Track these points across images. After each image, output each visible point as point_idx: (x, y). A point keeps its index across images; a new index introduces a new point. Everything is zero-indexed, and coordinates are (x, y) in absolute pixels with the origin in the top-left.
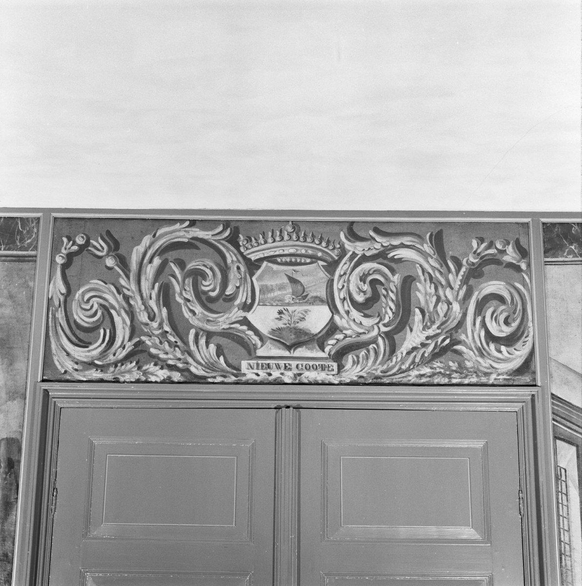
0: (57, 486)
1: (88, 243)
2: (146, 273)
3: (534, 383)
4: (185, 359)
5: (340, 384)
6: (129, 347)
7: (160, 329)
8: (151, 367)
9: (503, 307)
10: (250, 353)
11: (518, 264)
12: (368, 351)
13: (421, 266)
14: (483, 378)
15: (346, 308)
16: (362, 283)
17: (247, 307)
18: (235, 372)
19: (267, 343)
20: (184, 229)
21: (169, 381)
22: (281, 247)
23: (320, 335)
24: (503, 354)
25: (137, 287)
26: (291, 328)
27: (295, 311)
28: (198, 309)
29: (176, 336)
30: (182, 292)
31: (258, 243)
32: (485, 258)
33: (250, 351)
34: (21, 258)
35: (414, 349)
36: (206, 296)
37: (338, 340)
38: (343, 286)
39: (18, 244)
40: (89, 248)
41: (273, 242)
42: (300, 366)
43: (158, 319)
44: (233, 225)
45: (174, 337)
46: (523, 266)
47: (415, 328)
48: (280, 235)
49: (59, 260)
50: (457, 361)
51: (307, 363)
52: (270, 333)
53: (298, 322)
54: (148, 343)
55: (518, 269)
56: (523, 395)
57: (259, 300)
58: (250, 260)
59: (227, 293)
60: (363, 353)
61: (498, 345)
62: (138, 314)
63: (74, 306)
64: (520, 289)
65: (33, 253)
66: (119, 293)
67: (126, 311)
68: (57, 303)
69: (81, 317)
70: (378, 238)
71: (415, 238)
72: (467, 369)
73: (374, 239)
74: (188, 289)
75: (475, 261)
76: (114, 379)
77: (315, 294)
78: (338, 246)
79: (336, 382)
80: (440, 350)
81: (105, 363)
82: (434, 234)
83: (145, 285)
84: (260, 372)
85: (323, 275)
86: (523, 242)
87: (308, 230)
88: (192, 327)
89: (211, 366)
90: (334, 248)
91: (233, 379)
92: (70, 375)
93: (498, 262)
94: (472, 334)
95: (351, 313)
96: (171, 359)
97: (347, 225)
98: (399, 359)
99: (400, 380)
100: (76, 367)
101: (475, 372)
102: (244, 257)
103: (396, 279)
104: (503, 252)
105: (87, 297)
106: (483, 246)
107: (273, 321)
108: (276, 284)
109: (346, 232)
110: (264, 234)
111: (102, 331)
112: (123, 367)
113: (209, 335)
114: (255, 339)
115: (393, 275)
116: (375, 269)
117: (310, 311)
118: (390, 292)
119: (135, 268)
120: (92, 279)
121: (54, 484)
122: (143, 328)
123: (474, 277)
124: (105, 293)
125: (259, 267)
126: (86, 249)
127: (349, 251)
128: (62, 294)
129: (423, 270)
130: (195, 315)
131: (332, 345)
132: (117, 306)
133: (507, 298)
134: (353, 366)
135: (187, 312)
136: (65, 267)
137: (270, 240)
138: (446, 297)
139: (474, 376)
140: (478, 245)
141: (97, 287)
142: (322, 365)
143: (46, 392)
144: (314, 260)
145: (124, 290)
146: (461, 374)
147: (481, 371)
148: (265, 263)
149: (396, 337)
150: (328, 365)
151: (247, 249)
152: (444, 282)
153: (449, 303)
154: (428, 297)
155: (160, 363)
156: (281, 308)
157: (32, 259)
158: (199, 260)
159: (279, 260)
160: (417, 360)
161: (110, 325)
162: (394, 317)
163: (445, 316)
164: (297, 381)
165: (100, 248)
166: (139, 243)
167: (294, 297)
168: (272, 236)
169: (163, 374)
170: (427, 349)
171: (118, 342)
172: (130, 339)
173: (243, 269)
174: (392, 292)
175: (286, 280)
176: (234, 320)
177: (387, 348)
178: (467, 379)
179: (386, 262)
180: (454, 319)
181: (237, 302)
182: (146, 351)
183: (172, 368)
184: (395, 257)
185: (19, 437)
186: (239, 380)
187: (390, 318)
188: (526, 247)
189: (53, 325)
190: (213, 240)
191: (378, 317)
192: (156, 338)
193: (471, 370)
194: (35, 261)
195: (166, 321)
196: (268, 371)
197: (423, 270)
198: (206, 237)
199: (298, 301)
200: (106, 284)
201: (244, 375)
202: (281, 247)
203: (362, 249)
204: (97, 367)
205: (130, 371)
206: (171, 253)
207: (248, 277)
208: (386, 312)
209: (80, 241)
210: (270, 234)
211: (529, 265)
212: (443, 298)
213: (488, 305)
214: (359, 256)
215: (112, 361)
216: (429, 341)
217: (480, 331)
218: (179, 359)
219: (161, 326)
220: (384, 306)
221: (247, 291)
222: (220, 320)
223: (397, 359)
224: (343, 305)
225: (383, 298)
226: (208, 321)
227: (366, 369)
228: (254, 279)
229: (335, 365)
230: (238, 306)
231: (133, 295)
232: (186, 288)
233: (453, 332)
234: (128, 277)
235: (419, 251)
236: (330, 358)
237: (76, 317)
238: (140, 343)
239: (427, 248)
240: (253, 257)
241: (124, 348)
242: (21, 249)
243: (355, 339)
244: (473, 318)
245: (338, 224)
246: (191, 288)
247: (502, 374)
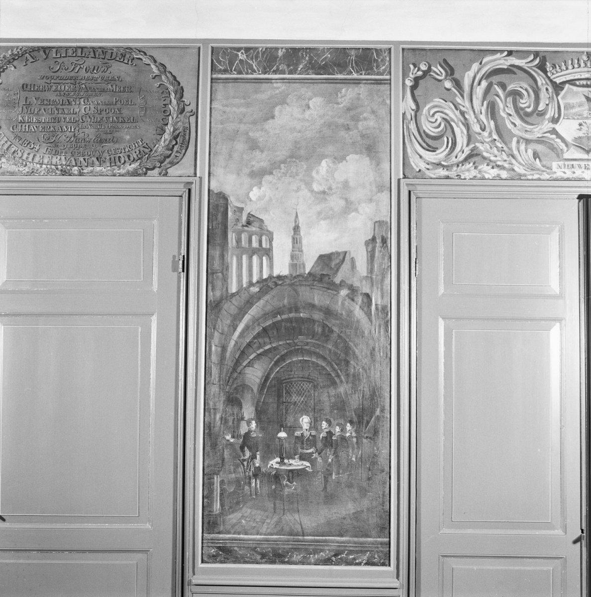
1: (429, 69)
2: (476, 94)
6: (467, 151)
8: (484, 167)
10: (558, 156)
17: (555, 120)
22: (579, 72)
25: (470, 103)
28: (518, 121)
29: (502, 143)
30: (505, 108)
33: (558, 154)
39: (375, 70)
43: (488, 129)
44: (541, 54)
48: (578, 63)
49: (409, 83)
52: (573, 140)
58: (555, 83)
59: (540, 109)
62: (472, 126)
65: (388, 77)
66: (457, 109)
67: (463, 124)
68: (409, 117)
69: (428, 128)
83: (477, 102)
84: (566, 171)
91: (548, 177)
96: (499, 161)
100: (428, 167)
102: (551, 81)
105: (432, 112)
108: (577, 103)
111: (445, 139)
112: (463, 167)
113: (528, 141)
114: (562, 146)
120: (435, 97)
122: (477, 137)
125: (562, 89)
128: (413, 110)
136: (414, 88)
137: (570, 67)
141: (439, 104)
145: (460, 106)
148: (567, 86)
151: (553, 74)
156: (581, 121)
158: (517, 83)
159: (578, 83)
166: (469, 69)
168: (572, 64)
172: (468, 145)
175: (584, 99)
176: (545, 131)
181: (547, 116)
189: (408, 134)
190: (527, 67)
195: (494, 132)
200: (446, 102)
202: (579, 72)
205: (468, 170)
206: (494, 77)
207: (555, 96)
209: (424, 67)
210: (570, 62)
219: (490, 134)
221: (555, 108)
222: (535, 130)
226: (526, 131)
228: (559, 97)
230: (549, 119)
232: (508, 105)
234: (462, 96)
237: (425, 128)
238: (475, 148)
240: (558, 81)
241: (463, 152)
242: (378, 74)
246: (512, 105)
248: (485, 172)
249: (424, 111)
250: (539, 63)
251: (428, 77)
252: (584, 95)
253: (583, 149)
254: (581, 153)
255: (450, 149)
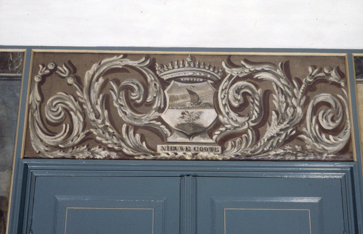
0: (33, 228)
1: (56, 69)
2: (94, 88)
3: (352, 160)
4: (120, 144)
5: (224, 160)
6: (82, 135)
7: (103, 124)
8: (97, 149)
9: (329, 110)
10: (163, 140)
11: (339, 82)
12: (242, 139)
13: (275, 84)
14: (318, 156)
15: (227, 110)
16: (237, 95)
17: (161, 110)
18: (153, 152)
19: (174, 133)
20: (120, 60)
21: (109, 158)
23: (210, 128)
24: (331, 141)
26: (190, 124)
27: (193, 112)
28: (128, 111)
30: (118, 101)
31: (168, 69)
32: (317, 79)
33: (163, 139)
34: (11, 78)
35: (272, 137)
36: (133, 103)
37: (222, 132)
38: (225, 96)
39: (10, 69)
40: (57, 72)
41: (177, 68)
42: (197, 148)
43: (102, 118)
45: (112, 129)
46: (342, 84)
47: (272, 124)
48: (183, 64)
49: (37, 79)
50: (301, 145)
51: (201, 146)
52: (176, 127)
53: (195, 120)
54: (95, 133)
55: (339, 86)
56: (344, 168)
57: (169, 105)
58: (163, 79)
59: (148, 101)
60: (238, 140)
61: (328, 134)
62: (88, 114)
63: (46, 109)
64: (341, 99)
65: (20, 75)
66: (76, 100)
67: (80, 113)
68: (34, 107)
69: (50, 117)
70: (247, 66)
71: (271, 66)
72: (307, 150)
73: (244, 66)
74: (122, 98)
75: (311, 80)
76: (72, 157)
77: (206, 102)
78: (221, 71)
79: (221, 159)
80: (289, 138)
81: (66, 146)
82: (284, 63)
83: (93, 95)
84: (170, 153)
85: (211, 89)
86: (342, 68)
87: (201, 60)
88: (124, 122)
89: (137, 148)
90: (218, 72)
91: (152, 156)
92: (44, 155)
93: (326, 81)
94: (310, 128)
95: (230, 114)
96: (110, 144)
97: (227, 57)
98: (262, 144)
99: (263, 157)
100: (47, 149)
101: (313, 153)
102: (159, 78)
103: (259, 91)
104: (329, 75)
105: (54, 103)
106: (316, 71)
107: (178, 119)
108: (180, 95)
109: (226, 62)
110: (172, 63)
111: (64, 126)
112: (78, 149)
113: (136, 129)
114: (166, 131)
115: (258, 89)
116: (245, 85)
117: (203, 113)
118: (256, 101)
119: (87, 85)
121: (30, 227)
122: (92, 123)
123: (311, 91)
124: (68, 101)
125: (169, 84)
126: (54, 72)
127: (228, 74)
128: (38, 101)
129: (277, 87)
130: (125, 114)
131: (218, 135)
132: (74, 109)
133: (332, 104)
134: (231, 148)
135: (121, 113)
136: (40, 84)
137: (176, 67)
138: (292, 103)
139: (312, 155)
140: (312, 70)
141: (62, 97)
142: (211, 148)
143: (26, 165)
144: (205, 79)
146: (303, 153)
147: (317, 152)
148: (173, 82)
149: (260, 129)
150: (215, 148)
151: (161, 72)
152: (291, 94)
153: (294, 108)
154: (281, 104)
155: (102, 146)
156: (183, 111)
157: (19, 79)
158: (128, 80)
159: (182, 79)
160: (274, 145)
161: (70, 122)
162: (258, 116)
163: (292, 116)
164: (195, 158)
165: (63, 71)
166: (89, 68)
167: (192, 103)
168: (177, 64)
169: (104, 153)
170: (281, 137)
171: (75, 133)
172: (83, 131)
173: (158, 85)
174: (257, 100)
175: (187, 93)
176: (152, 118)
177: (254, 137)
178: (308, 157)
179: (252, 81)
180: (298, 118)
181: (155, 106)
182: (94, 138)
183: (111, 150)
184: (259, 78)
185: (7, 196)
186: (155, 158)
187: (256, 117)
188: (343, 71)
189: (32, 121)
190: (139, 67)
191: (248, 116)
192: (100, 130)
193: (310, 151)
194: (21, 80)
196: (175, 151)
197: (277, 87)
198: (134, 65)
199: (195, 106)
200: (67, 94)
201: (159, 154)
203: (237, 73)
204: (61, 149)
205: (82, 152)
207: (162, 90)
208: (253, 114)
209: (51, 67)
210: (176, 63)
211: (346, 83)
212: (290, 104)
213: (320, 109)
214: (234, 77)
215: (71, 145)
216: (282, 132)
217: (315, 125)
218: (116, 144)
219: (103, 122)
220: (252, 109)
221: (161, 100)
222: (143, 118)
223: (261, 143)
224: (225, 109)
225: (251, 105)
226: (135, 119)
227: (240, 150)
228: (165, 92)
229: (220, 148)
230: (155, 109)
231: (85, 102)
233: (298, 126)
234: (82, 90)
235: (274, 74)
236: (216, 143)
237: (47, 116)
238: (90, 133)
239: (279, 72)
240: (165, 78)
241: (79, 136)
242: (12, 72)
243: (233, 131)
244: (310, 117)
245: (221, 57)
247: (331, 154)
248: (97, 154)
249: (48, 102)
250: (149, 63)
251: (54, 74)
252: (187, 90)
253: (185, 134)
254: (183, 137)
255: (68, 134)
